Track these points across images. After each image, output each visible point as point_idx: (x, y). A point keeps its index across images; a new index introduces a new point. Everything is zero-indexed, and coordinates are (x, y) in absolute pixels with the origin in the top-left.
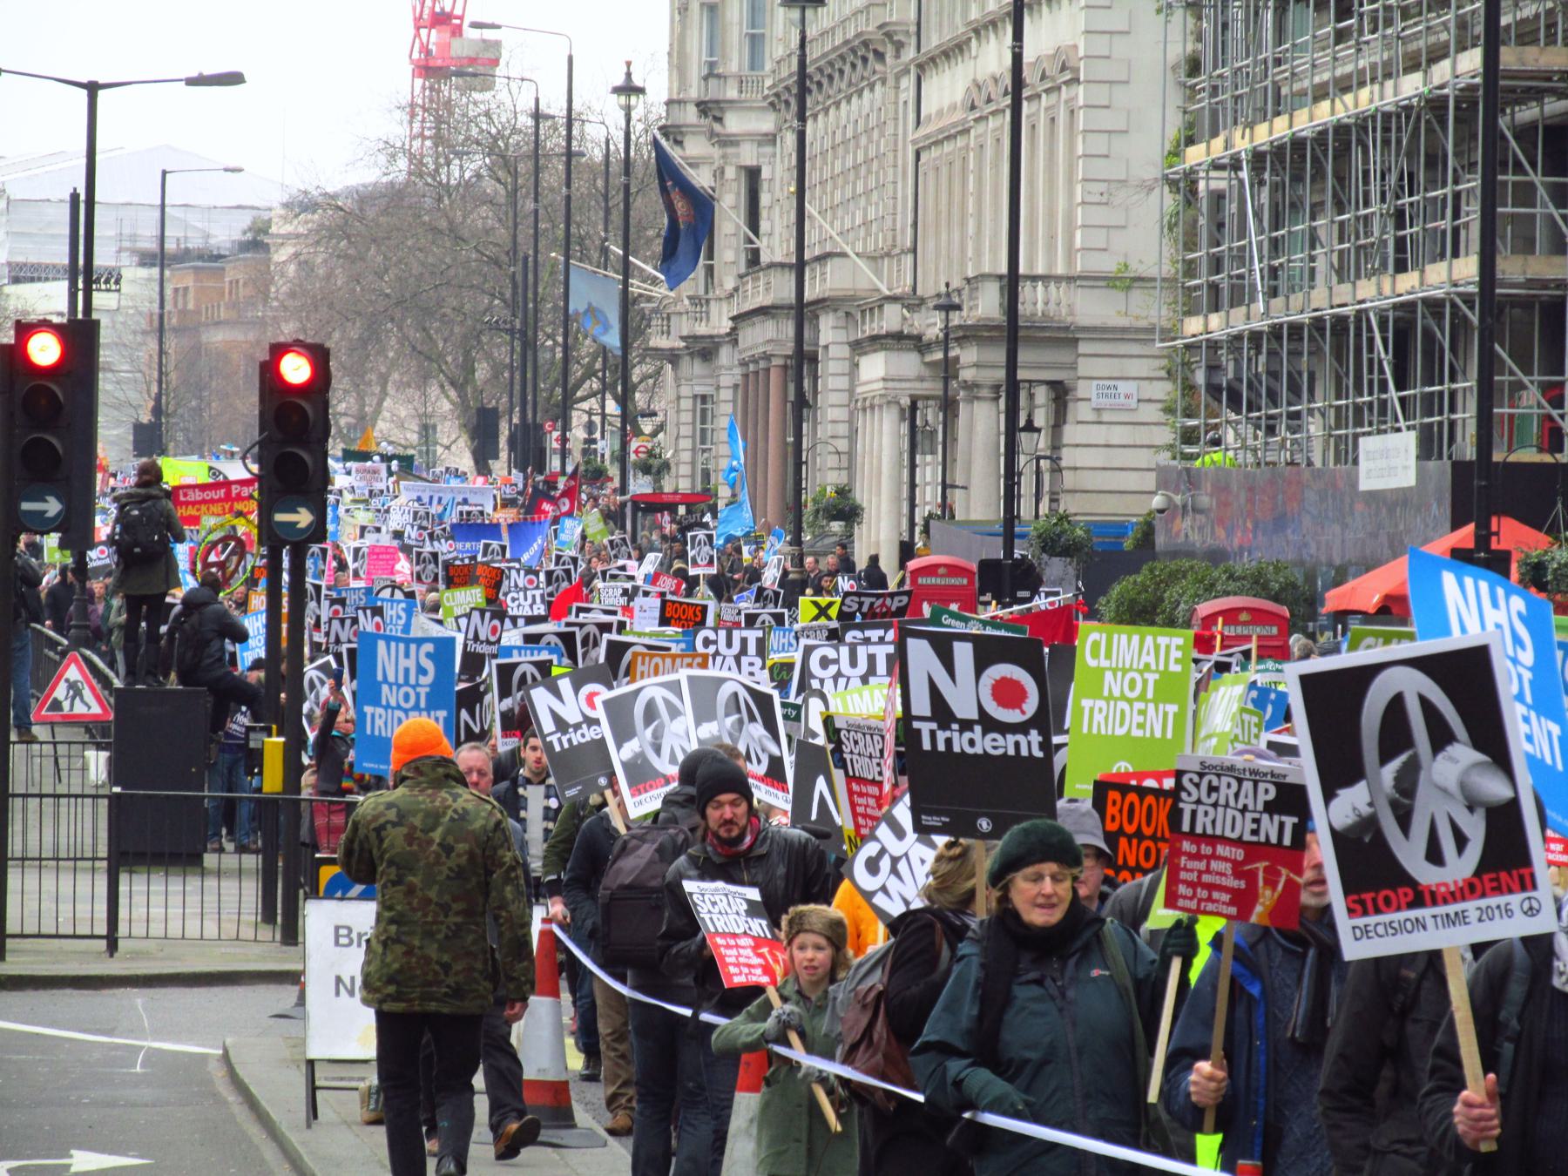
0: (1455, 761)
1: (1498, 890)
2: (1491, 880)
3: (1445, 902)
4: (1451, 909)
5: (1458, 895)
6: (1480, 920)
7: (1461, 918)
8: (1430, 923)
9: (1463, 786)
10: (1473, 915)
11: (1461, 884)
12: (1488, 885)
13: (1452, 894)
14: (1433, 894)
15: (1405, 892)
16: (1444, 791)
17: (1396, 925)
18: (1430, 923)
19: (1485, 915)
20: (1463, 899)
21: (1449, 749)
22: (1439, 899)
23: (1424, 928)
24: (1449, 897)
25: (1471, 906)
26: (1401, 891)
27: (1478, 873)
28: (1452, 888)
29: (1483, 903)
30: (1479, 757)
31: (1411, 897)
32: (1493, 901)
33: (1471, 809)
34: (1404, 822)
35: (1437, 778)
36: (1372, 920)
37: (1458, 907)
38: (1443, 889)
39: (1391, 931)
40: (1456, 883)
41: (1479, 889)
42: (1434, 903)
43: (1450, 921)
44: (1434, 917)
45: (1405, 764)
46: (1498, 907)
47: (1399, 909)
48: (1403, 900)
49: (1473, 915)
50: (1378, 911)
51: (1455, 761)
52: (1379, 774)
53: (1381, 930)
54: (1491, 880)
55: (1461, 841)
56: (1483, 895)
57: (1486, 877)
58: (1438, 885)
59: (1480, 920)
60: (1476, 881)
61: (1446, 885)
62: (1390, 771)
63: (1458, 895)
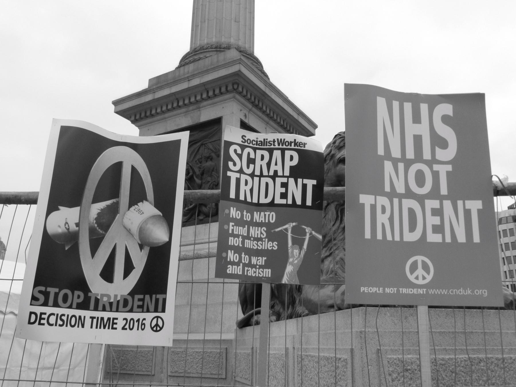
0: (141, 212)
1: (142, 308)
2: (139, 300)
3: (104, 310)
4: (106, 315)
5: (114, 307)
6: (124, 328)
7: (111, 324)
8: (88, 322)
9: (141, 230)
10: (120, 323)
11: (119, 298)
12: (137, 303)
13: (111, 304)
14: (97, 301)
15: (79, 296)
16: (129, 231)
17: (65, 318)
18: (88, 322)
19: (129, 325)
20: (117, 311)
21: (140, 204)
22: (100, 307)
23: (83, 326)
24: (108, 307)
25: (121, 316)
26: (77, 293)
27: (132, 293)
28: (112, 300)
29: (129, 316)
30: (157, 212)
31: (81, 300)
32: (136, 316)
33: (141, 247)
34: (95, 246)
35: (126, 222)
36: (48, 310)
37: (112, 315)
38: (105, 299)
39: (60, 322)
40: (116, 296)
41: (129, 307)
42: (96, 309)
43: (103, 324)
44: (92, 318)
45: (108, 206)
46: (138, 320)
47: (70, 307)
48: (76, 301)
49: (120, 323)
50: (56, 305)
51: (141, 212)
52: (90, 207)
53: (52, 320)
54: (139, 300)
55: (129, 268)
56: (131, 311)
57: (137, 297)
58: (103, 295)
59: (124, 328)
60: (130, 299)
61: (108, 296)
62: (97, 208)
63: (114, 307)
